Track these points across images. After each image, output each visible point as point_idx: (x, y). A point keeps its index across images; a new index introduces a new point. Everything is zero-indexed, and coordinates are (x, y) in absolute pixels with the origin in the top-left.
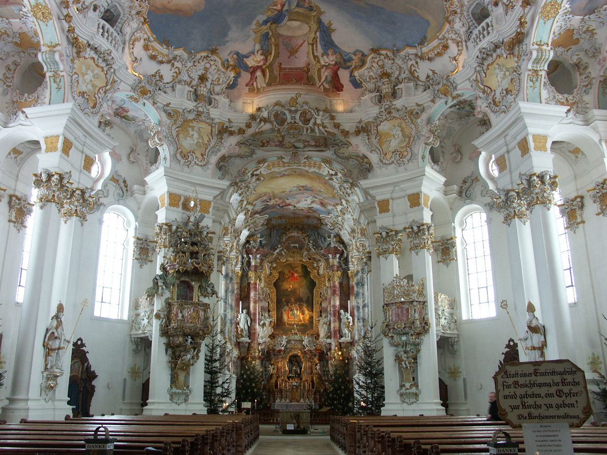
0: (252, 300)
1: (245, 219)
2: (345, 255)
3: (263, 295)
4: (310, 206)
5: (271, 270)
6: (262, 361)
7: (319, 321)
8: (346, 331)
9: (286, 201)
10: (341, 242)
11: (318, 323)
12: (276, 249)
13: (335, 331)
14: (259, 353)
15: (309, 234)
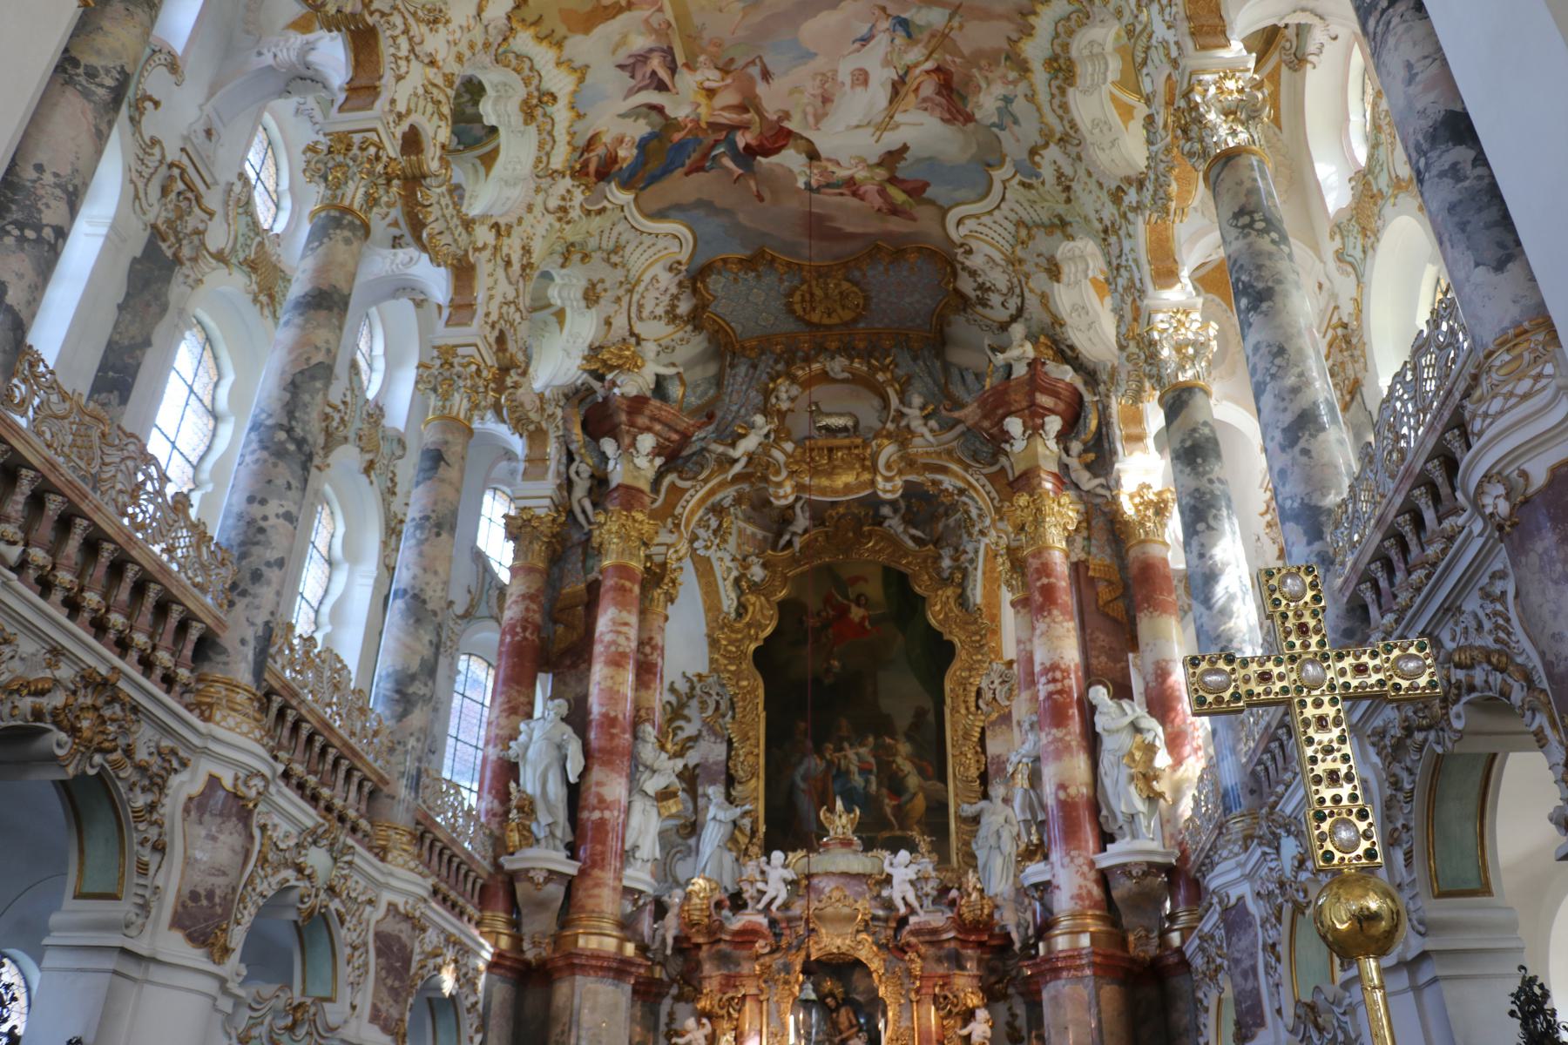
0: (598, 649)
1: (544, 173)
2: (1093, 424)
3: (703, 706)
4: (892, 140)
5: (741, 593)
6: (647, 994)
7: (976, 820)
8: (1126, 799)
9: (761, 89)
10: (1069, 355)
11: (974, 834)
12: (743, 436)
13: (1067, 807)
14: (622, 940)
15: (900, 372)
